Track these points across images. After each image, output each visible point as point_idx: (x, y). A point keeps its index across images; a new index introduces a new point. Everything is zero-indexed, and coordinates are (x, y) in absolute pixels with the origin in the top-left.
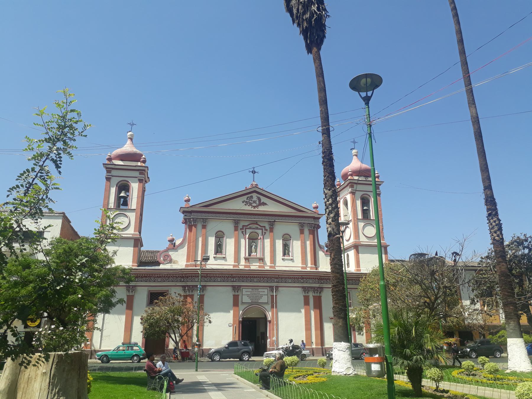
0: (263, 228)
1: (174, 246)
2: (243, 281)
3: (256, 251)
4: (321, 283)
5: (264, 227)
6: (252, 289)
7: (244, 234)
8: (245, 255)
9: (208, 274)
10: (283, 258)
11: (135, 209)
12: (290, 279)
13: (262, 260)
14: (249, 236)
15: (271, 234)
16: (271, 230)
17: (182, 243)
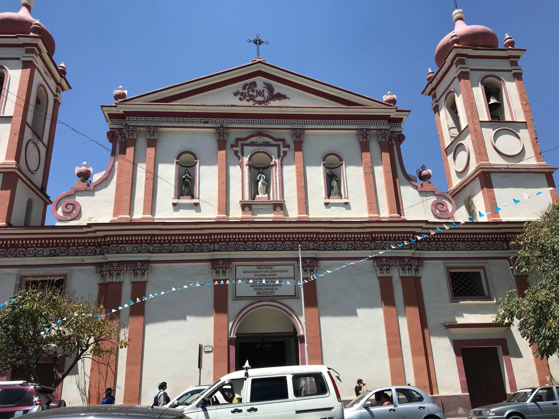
0: (281, 143)
1: (88, 186)
2: (236, 250)
3: (267, 191)
4: (418, 249)
5: (283, 140)
6: (259, 267)
7: (239, 155)
8: (243, 198)
9: (154, 235)
10: (327, 201)
11: (11, 117)
12: (345, 241)
13: (279, 206)
14: (250, 159)
15: (299, 154)
16: (299, 147)
17: (106, 178)
